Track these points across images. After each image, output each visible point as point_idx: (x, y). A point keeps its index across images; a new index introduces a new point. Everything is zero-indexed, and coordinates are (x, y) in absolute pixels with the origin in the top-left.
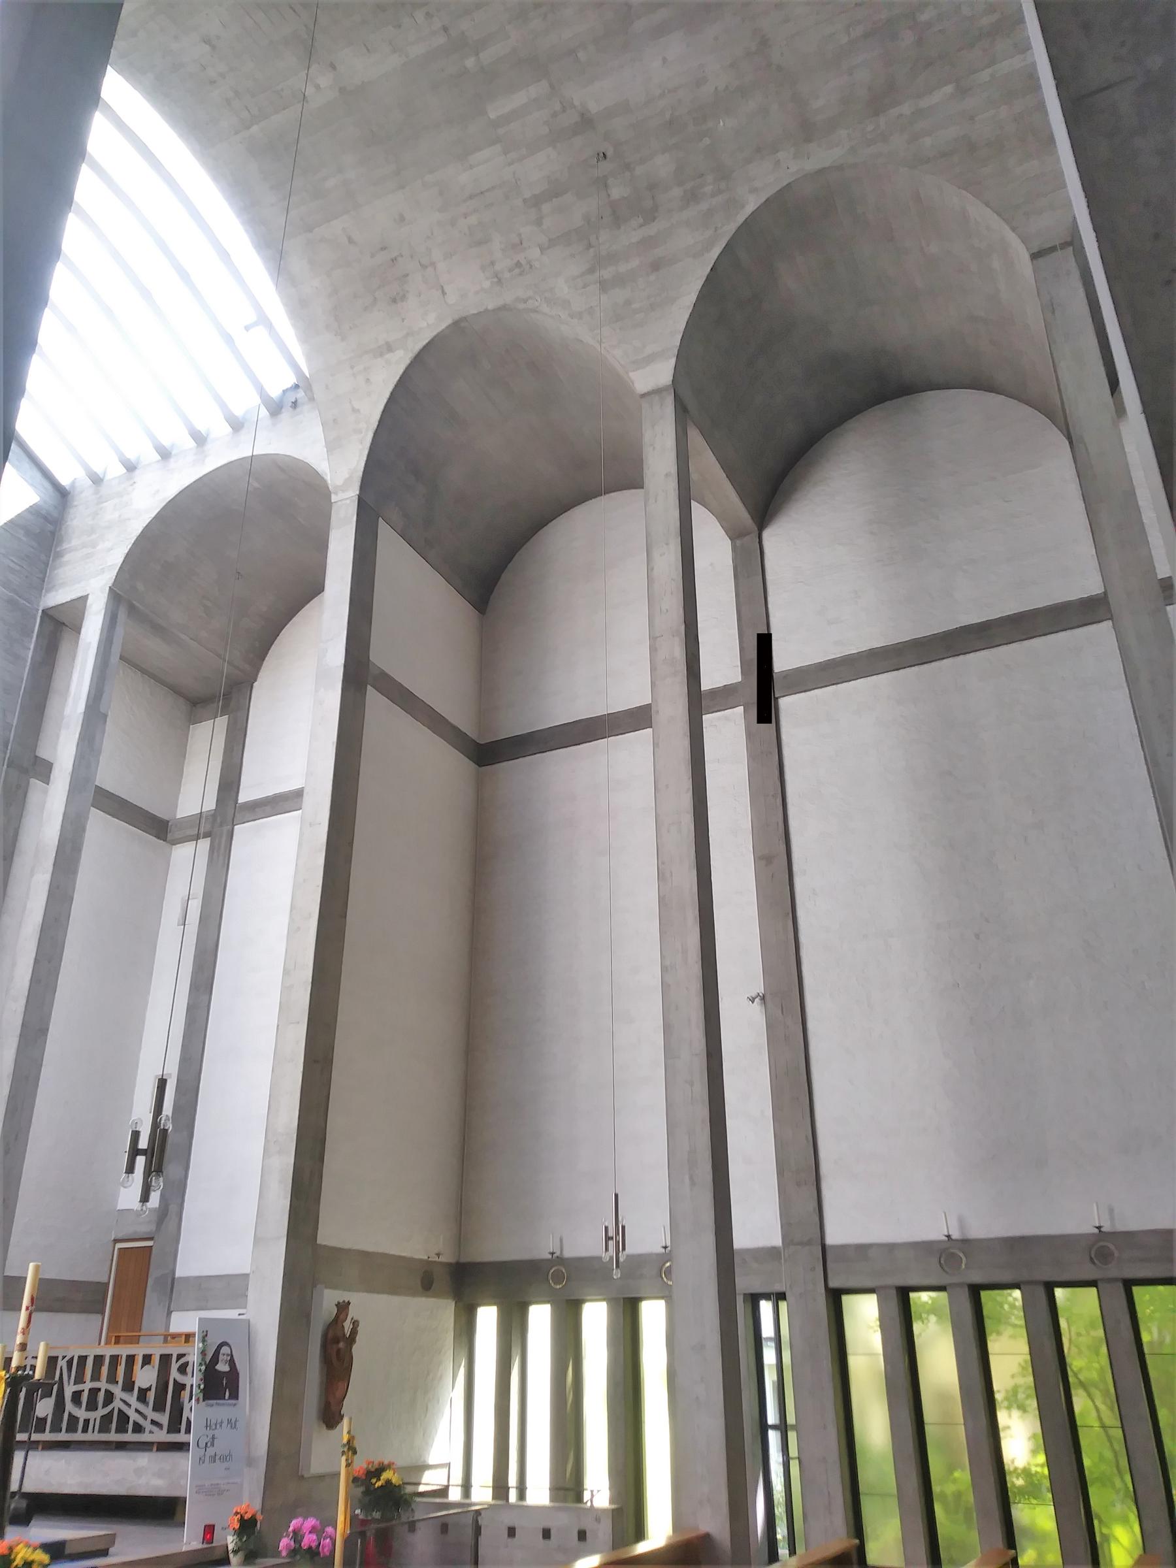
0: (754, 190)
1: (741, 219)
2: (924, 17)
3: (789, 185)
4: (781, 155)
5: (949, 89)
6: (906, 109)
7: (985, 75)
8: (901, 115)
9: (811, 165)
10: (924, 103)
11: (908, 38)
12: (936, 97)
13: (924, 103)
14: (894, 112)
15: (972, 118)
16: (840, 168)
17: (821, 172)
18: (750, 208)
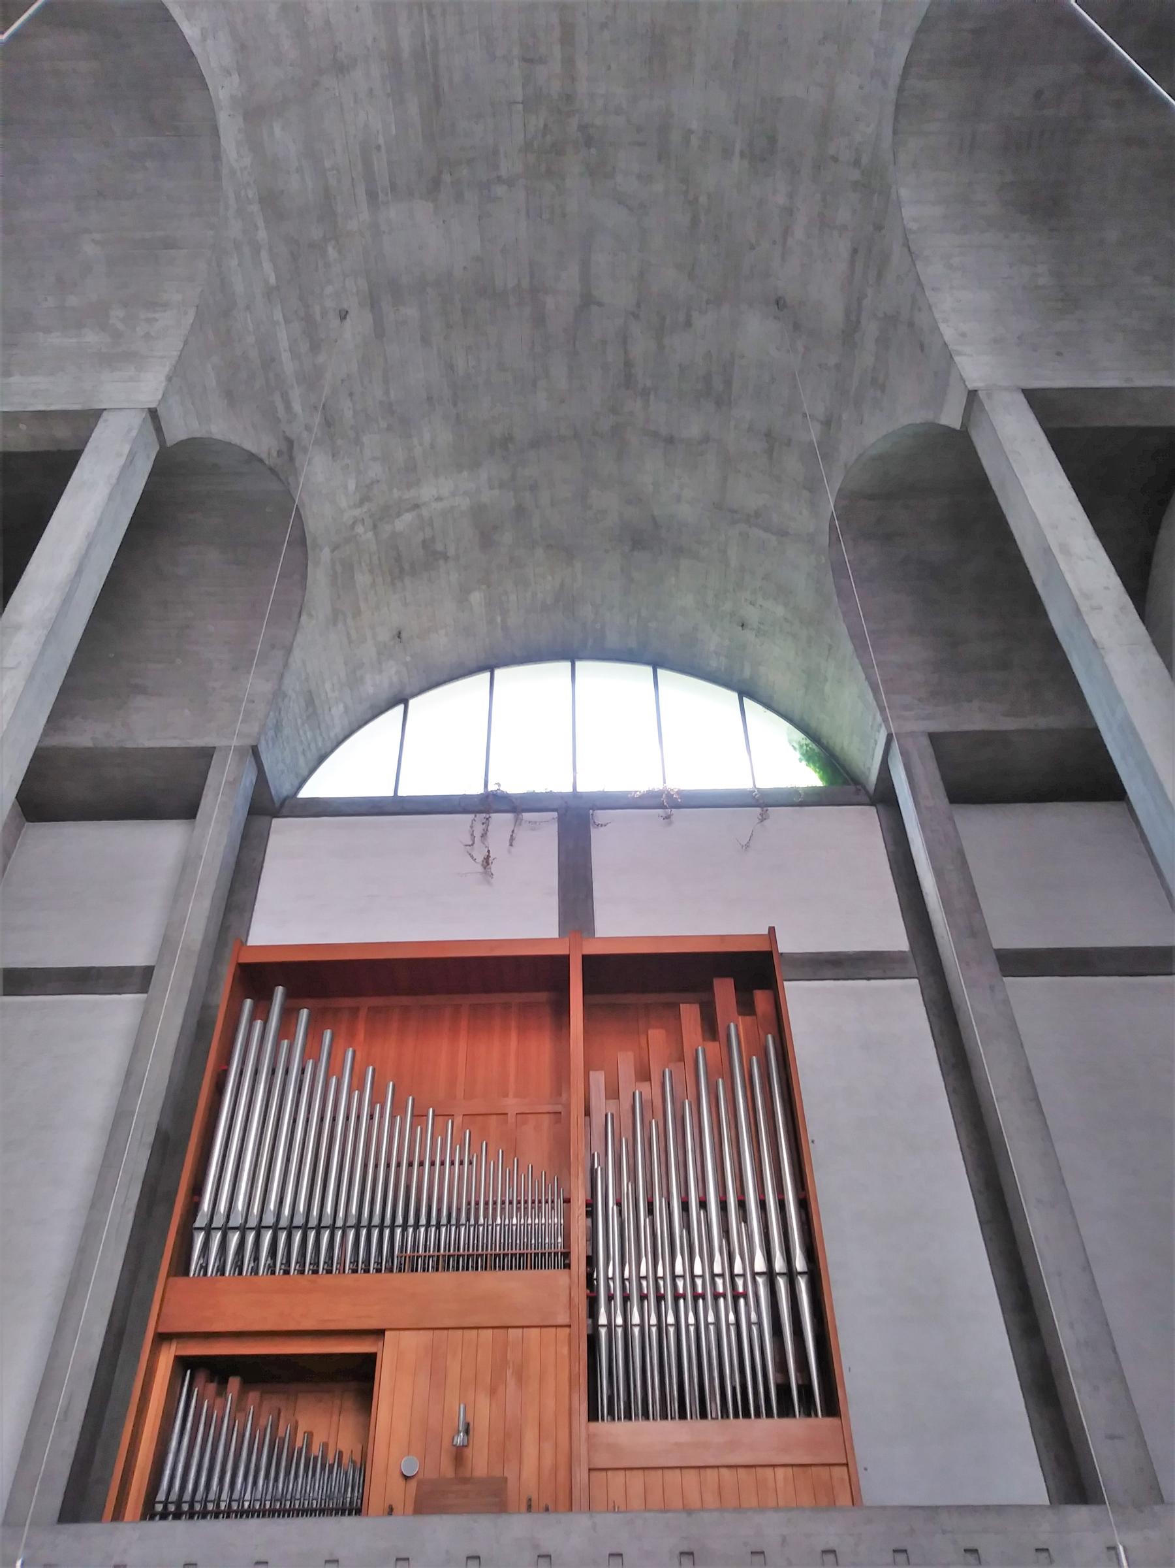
0: (204, 38)
1: (177, 13)
2: (332, 252)
3: (205, 87)
4: (235, 78)
5: (272, 280)
6: (262, 235)
7: (278, 316)
8: (257, 230)
9: (223, 118)
10: (264, 254)
11: (316, 233)
12: (267, 266)
13: (264, 254)
14: (261, 223)
15: (248, 308)
16: (217, 157)
17: (215, 131)
18: (190, 30)
